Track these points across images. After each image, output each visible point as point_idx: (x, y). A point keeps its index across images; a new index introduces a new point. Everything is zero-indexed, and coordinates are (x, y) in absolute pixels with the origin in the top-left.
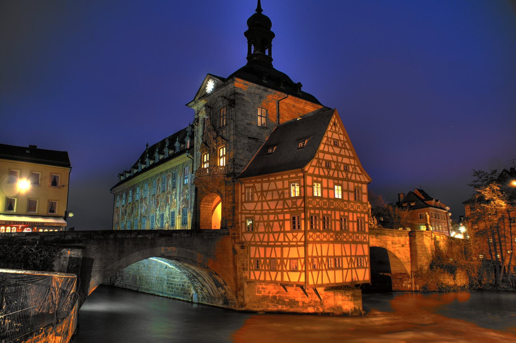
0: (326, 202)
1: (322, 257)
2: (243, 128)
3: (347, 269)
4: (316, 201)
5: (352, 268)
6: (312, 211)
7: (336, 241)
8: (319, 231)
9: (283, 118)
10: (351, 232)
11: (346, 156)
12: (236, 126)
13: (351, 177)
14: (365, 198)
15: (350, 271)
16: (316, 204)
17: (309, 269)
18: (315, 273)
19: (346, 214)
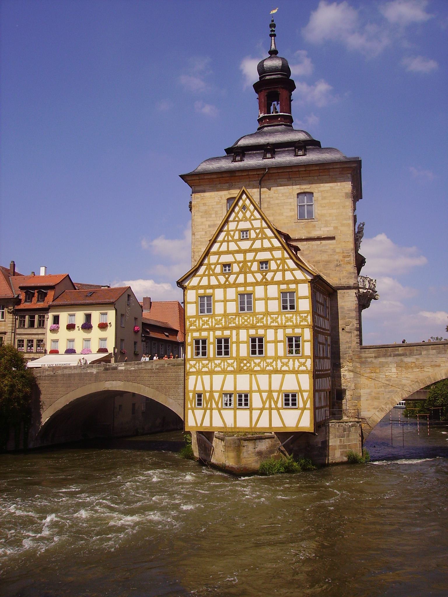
0: (221, 320)
1: (211, 392)
2: (204, 233)
3: (262, 410)
4: (203, 321)
5: (270, 409)
6: (196, 335)
7: (240, 371)
8: (209, 359)
9: (269, 202)
10: (270, 358)
11: (263, 249)
12: (193, 234)
13: (273, 278)
14: (304, 305)
15: (266, 413)
16: (203, 325)
17: (189, 406)
18: (199, 413)
19: (261, 332)
